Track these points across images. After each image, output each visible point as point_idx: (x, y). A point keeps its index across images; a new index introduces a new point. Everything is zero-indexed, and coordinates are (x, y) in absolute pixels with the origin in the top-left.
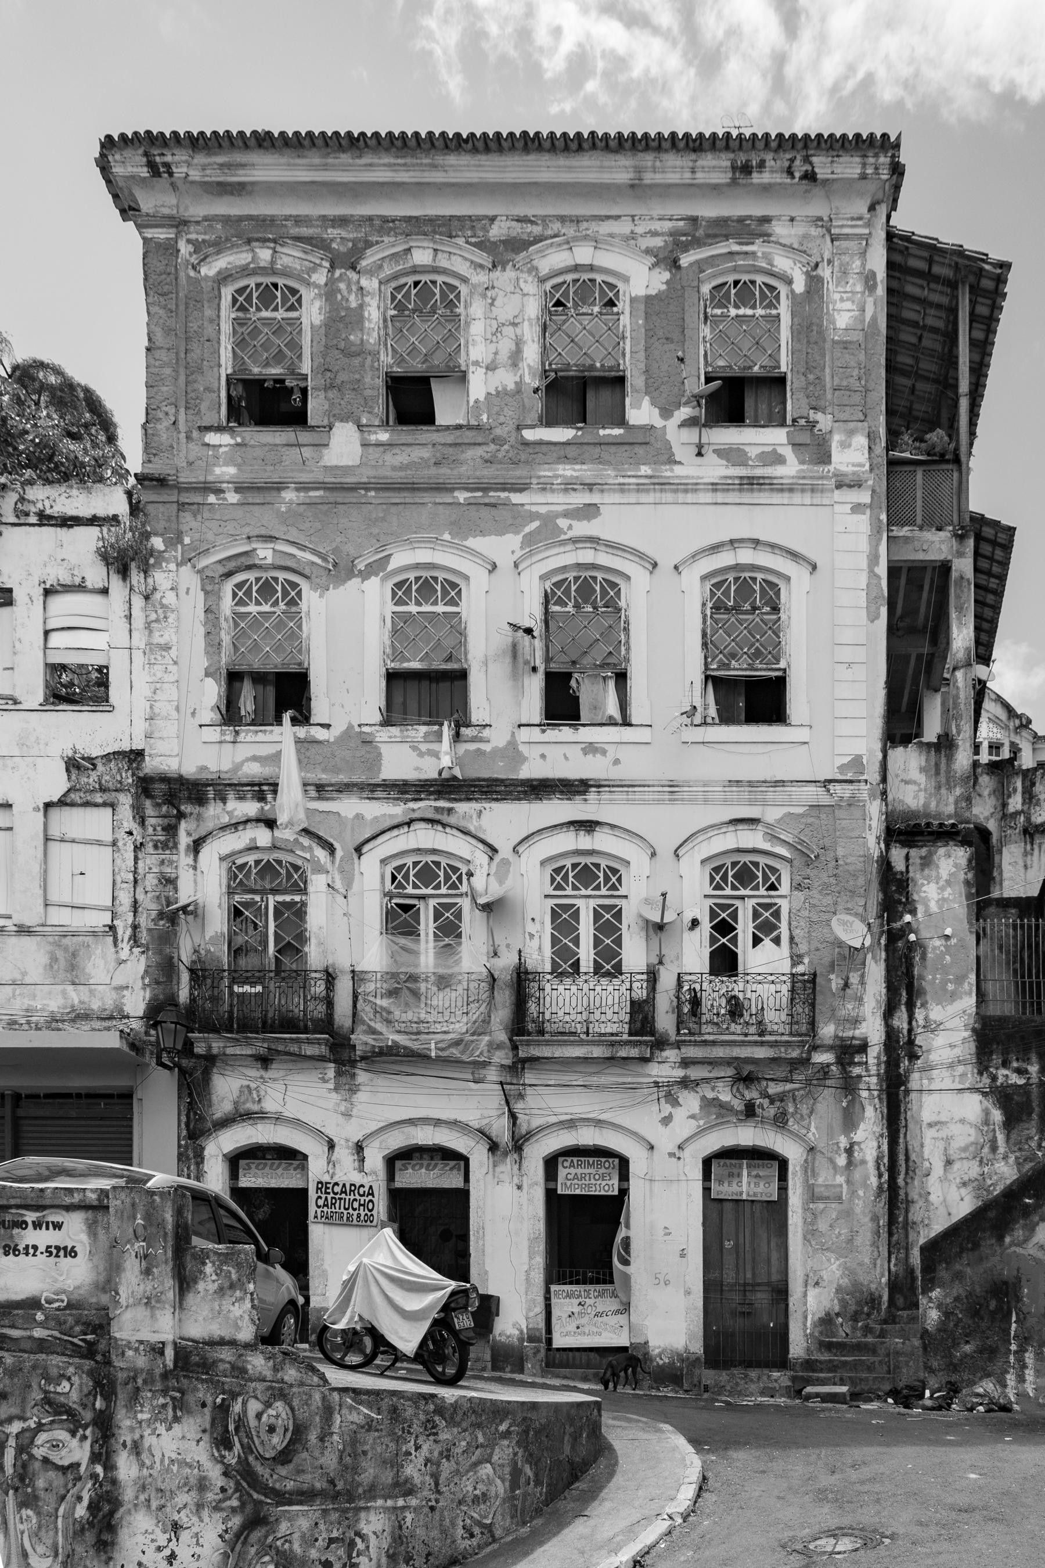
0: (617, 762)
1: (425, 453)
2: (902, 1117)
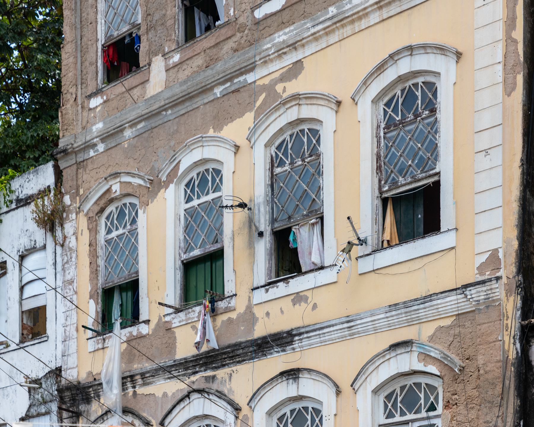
0: (315, 306)
1: (199, 61)
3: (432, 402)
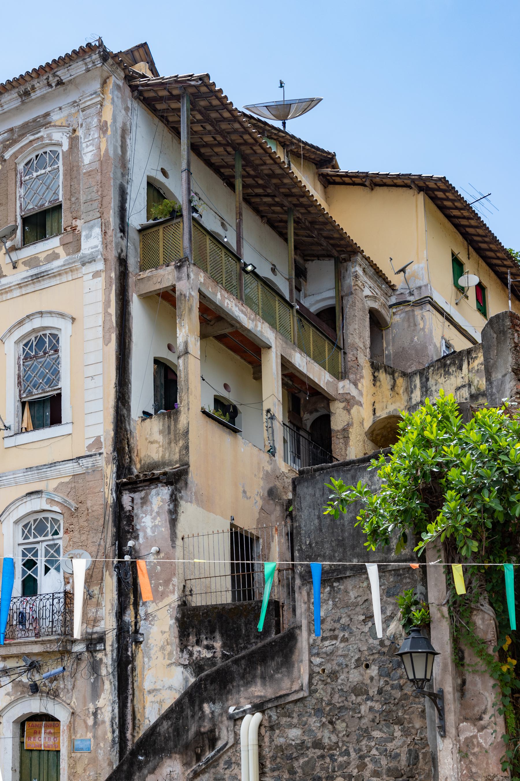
2: (130, 687)
3: (56, 530)
